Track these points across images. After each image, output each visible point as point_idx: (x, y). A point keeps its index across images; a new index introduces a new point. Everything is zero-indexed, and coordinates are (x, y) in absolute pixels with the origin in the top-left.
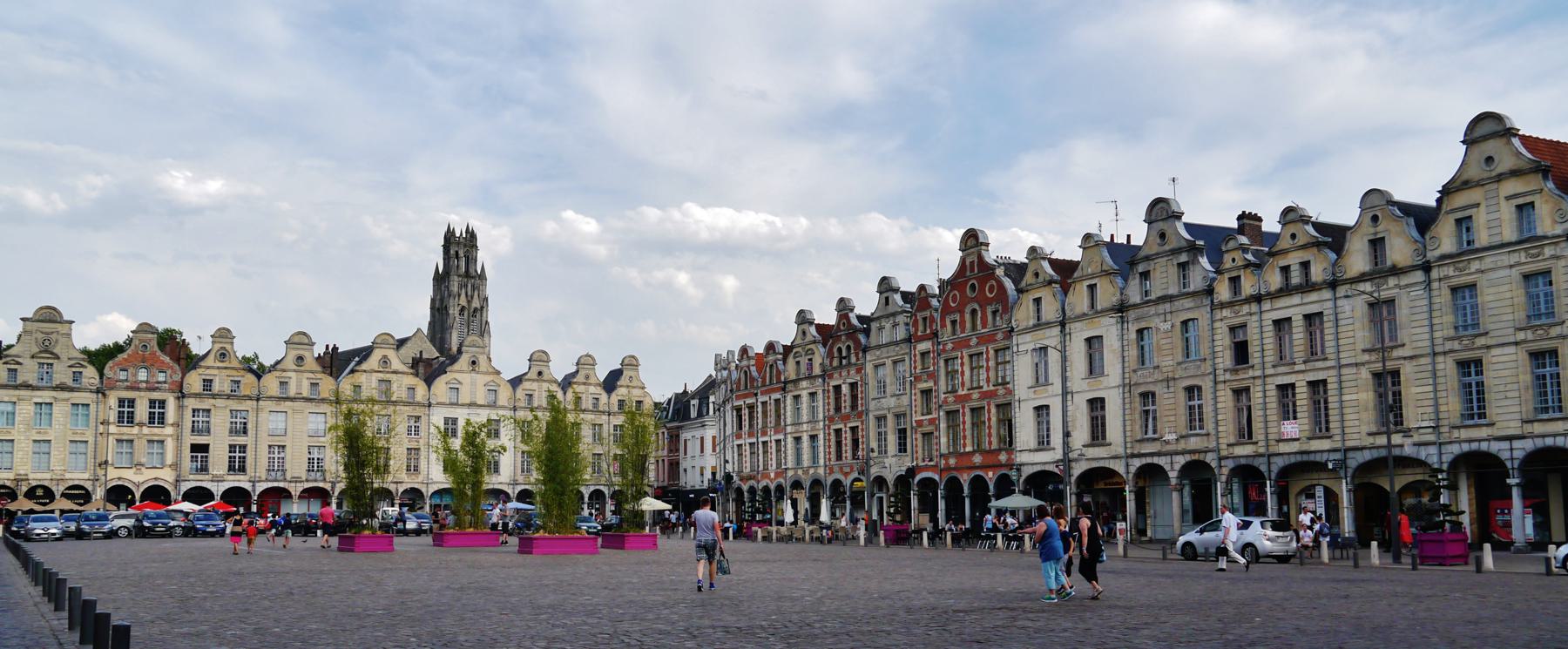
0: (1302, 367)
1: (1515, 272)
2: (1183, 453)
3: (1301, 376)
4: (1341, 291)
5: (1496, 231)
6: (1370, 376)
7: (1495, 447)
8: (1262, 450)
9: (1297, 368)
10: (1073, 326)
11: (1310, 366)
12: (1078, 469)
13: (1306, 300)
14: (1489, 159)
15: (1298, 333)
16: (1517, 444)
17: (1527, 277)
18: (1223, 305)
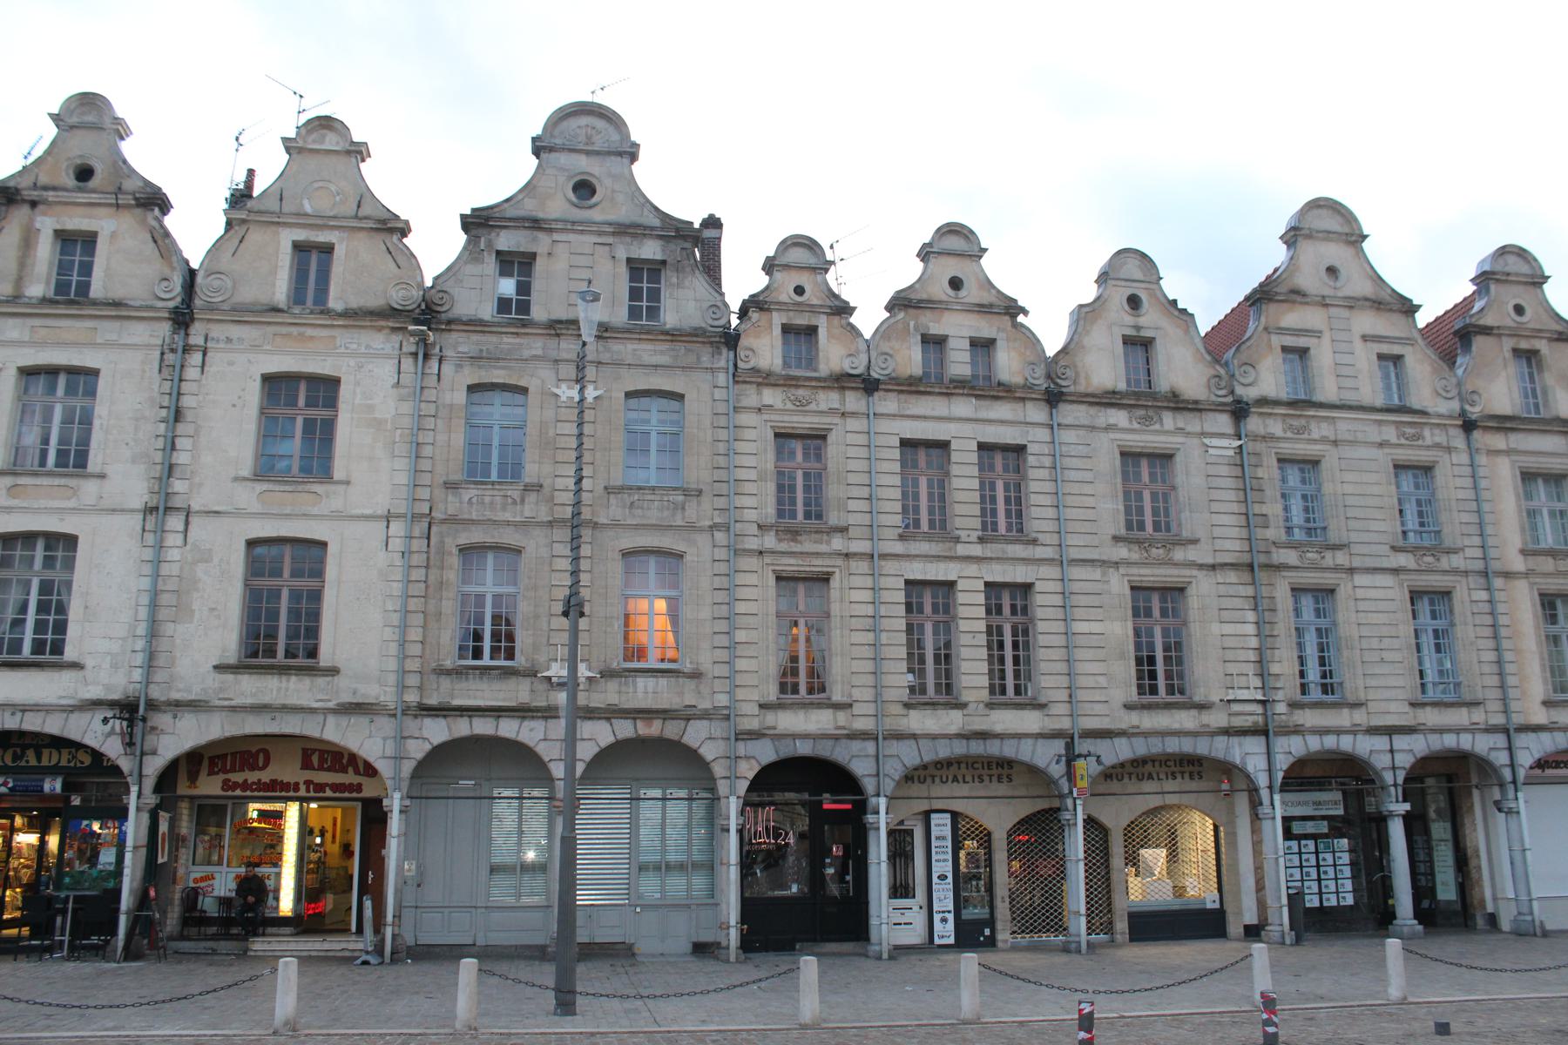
0: (977, 550)
1: (1384, 458)
2: (610, 714)
3: (972, 569)
4: (1070, 413)
5: (1348, 383)
6: (1128, 591)
7: (1364, 746)
8: (861, 724)
9: (961, 550)
10: (217, 331)
11: (990, 550)
12: (177, 737)
13: (983, 414)
14: (1332, 271)
15: (965, 477)
16: (1401, 742)
17: (1399, 467)
18: (765, 379)
